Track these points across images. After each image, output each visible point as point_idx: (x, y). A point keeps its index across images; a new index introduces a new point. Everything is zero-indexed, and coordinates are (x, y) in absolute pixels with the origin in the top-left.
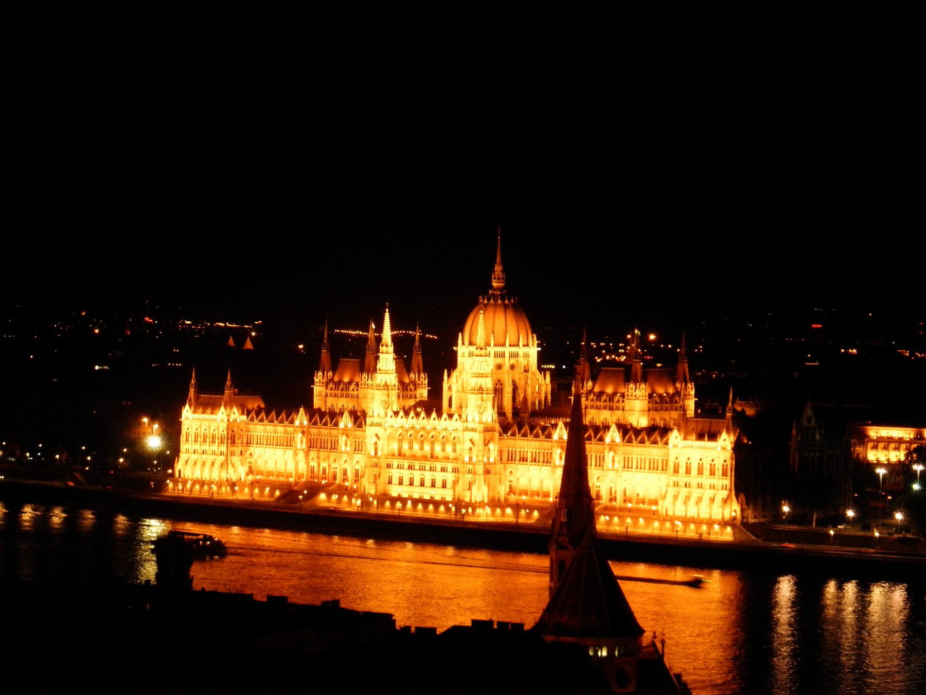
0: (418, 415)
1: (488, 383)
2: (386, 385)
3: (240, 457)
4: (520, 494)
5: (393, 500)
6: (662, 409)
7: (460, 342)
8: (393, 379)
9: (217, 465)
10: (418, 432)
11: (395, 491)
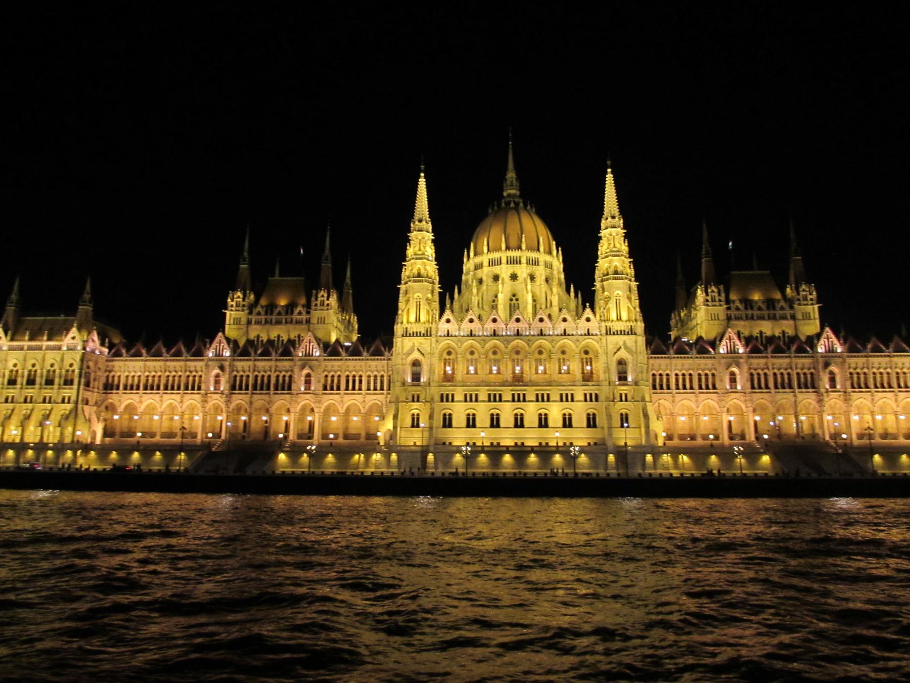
8: (431, 268)
10: (509, 342)
11: (459, 437)
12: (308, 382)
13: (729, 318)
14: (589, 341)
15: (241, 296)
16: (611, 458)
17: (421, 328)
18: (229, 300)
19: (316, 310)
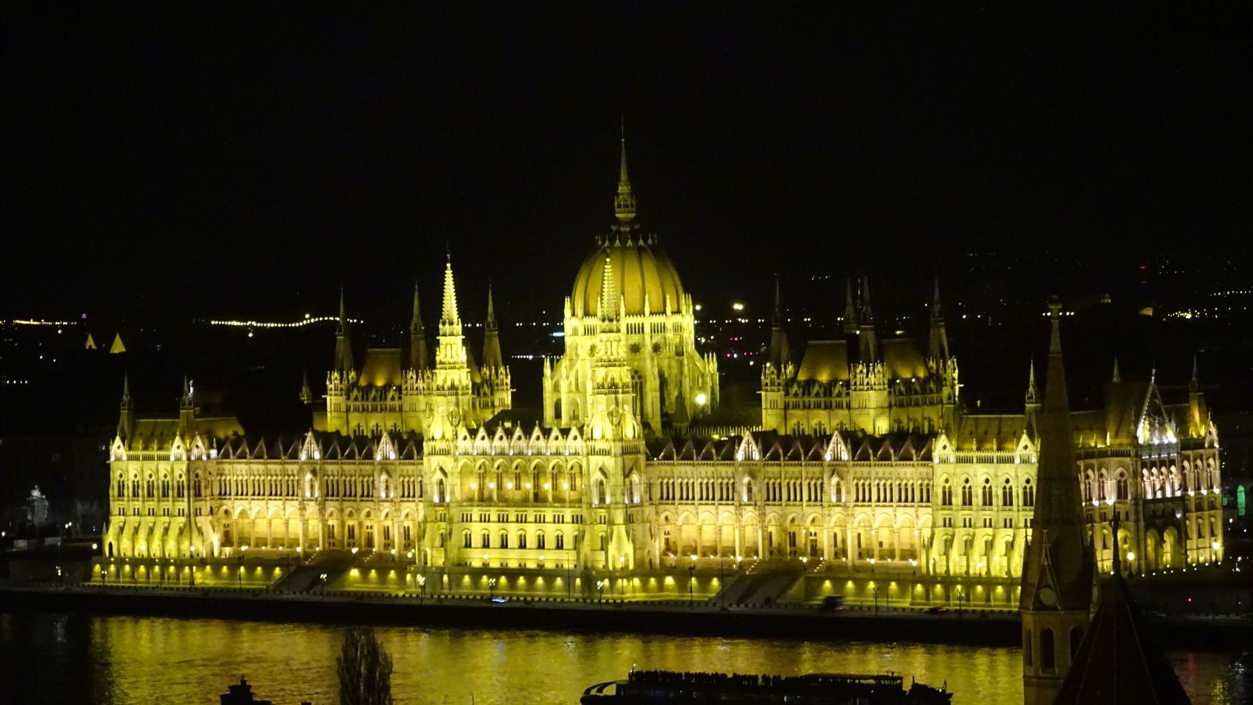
0: (509, 433)
1: (622, 375)
2: (453, 387)
3: (210, 518)
4: (685, 553)
5: (477, 574)
6: (909, 405)
7: (567, 312)
8: (462, 377)
9: (174, 532)
10: (512, 461)
11: (477, 558)
12: (387, 488)
13: (786, 407)
16: (578, 581)
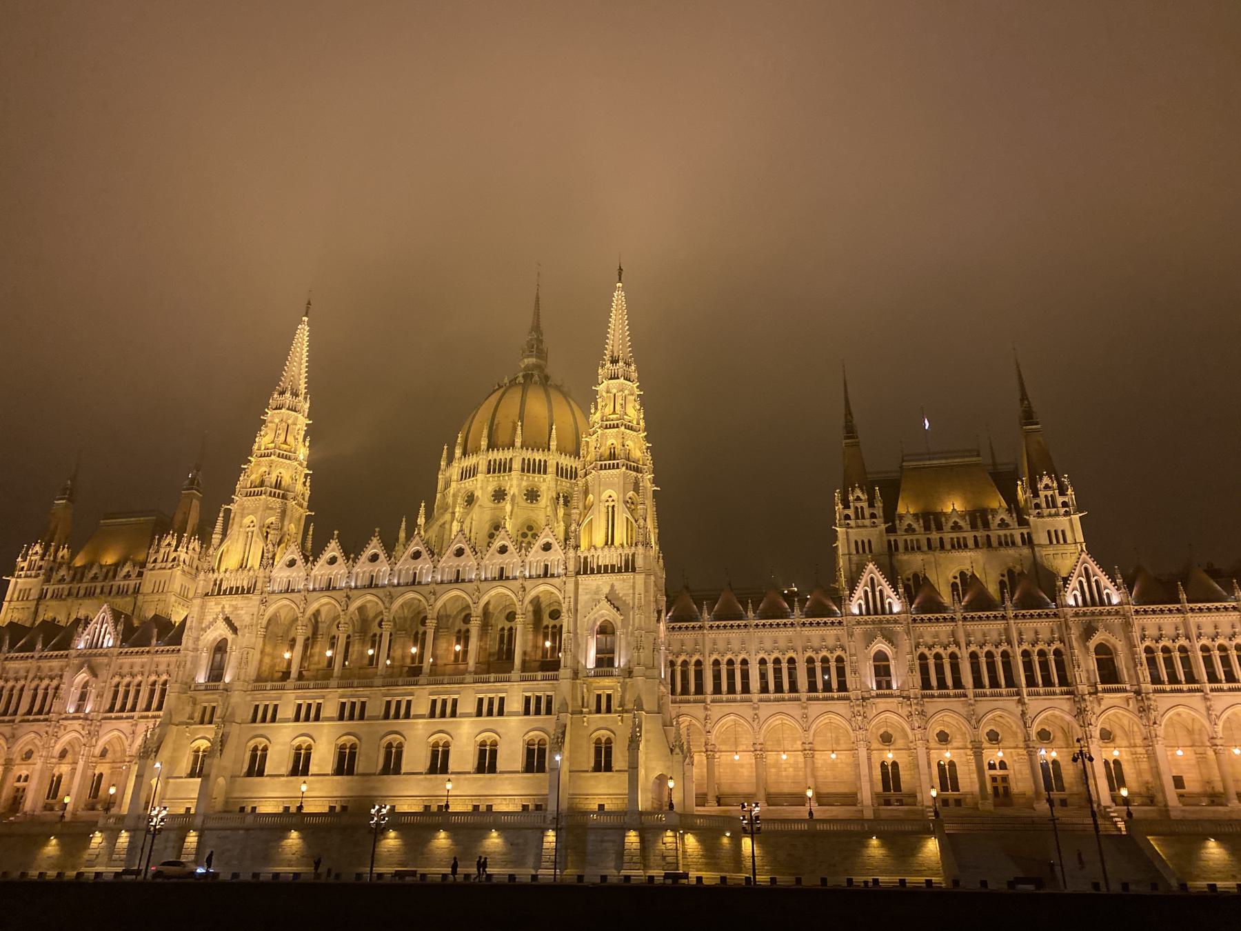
2: (278, 485)
10: (392, 598)
11: (271, 796)
12: (83, 697)
13: (892, 548)
14: (542, 588)
15: (40, 552)
16: (551, 836)
17: (242, 580)
18: (19, 559)
19: (153, 569)
